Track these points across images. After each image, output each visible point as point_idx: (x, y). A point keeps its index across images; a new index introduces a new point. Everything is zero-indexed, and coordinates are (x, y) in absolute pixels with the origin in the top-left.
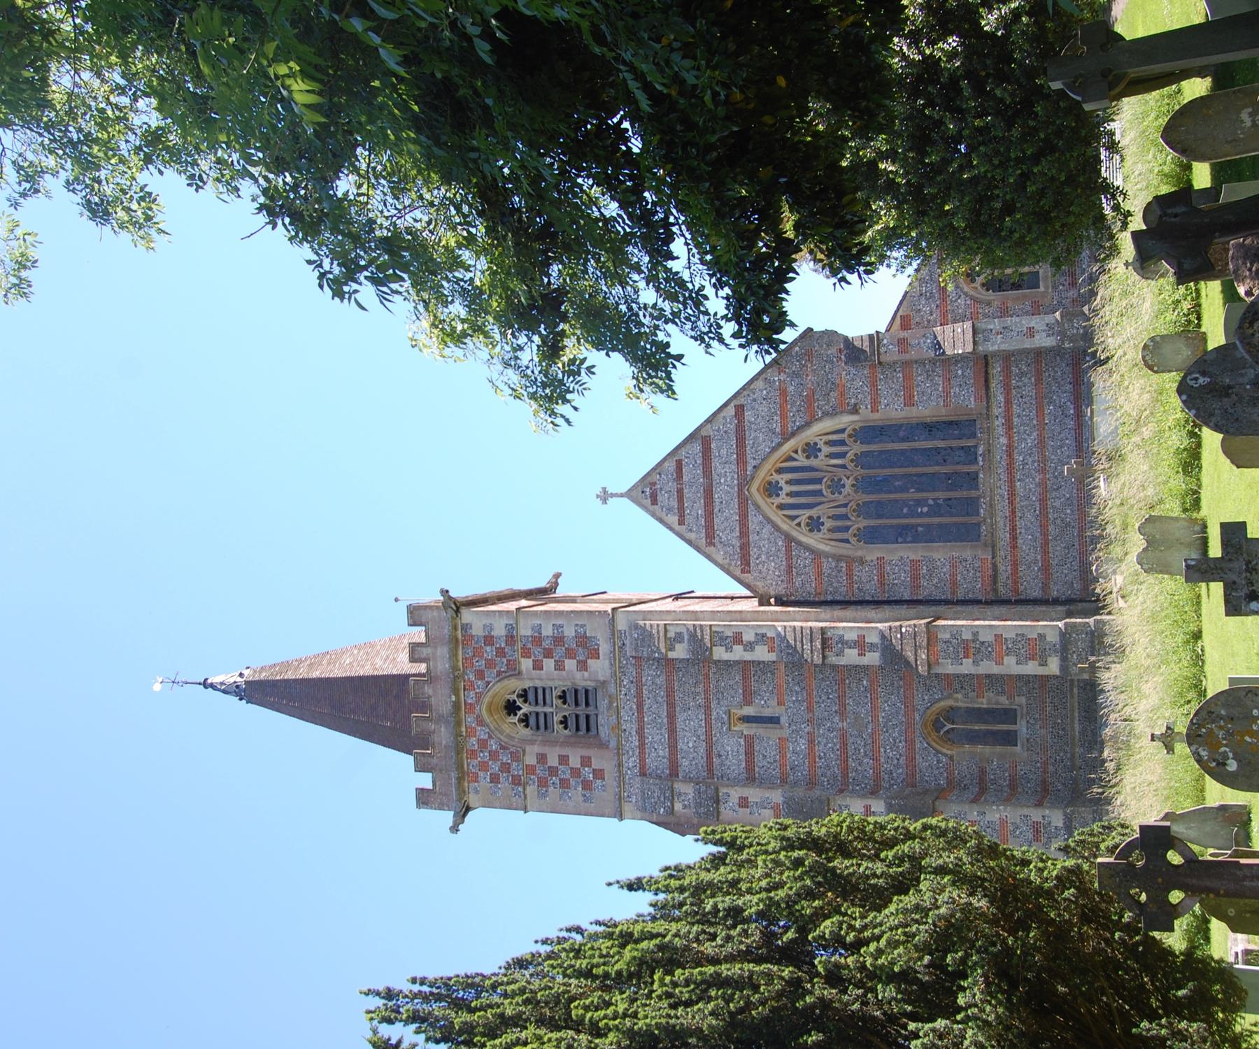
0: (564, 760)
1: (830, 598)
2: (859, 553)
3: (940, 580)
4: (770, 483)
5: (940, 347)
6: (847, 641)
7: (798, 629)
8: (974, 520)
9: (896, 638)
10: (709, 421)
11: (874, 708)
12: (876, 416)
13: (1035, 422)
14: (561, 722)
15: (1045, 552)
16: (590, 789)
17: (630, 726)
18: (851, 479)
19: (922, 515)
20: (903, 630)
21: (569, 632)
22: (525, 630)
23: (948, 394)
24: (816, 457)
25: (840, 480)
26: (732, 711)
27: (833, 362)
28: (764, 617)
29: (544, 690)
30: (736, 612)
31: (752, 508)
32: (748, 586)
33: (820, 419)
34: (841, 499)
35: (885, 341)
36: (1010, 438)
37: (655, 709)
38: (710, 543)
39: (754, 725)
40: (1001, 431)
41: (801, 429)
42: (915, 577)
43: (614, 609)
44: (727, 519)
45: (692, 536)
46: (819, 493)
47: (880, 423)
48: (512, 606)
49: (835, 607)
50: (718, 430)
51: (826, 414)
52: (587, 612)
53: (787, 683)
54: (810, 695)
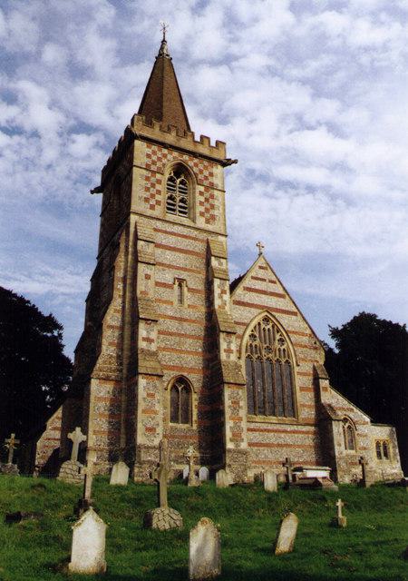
11: (189, 353)
37: (183, 244)
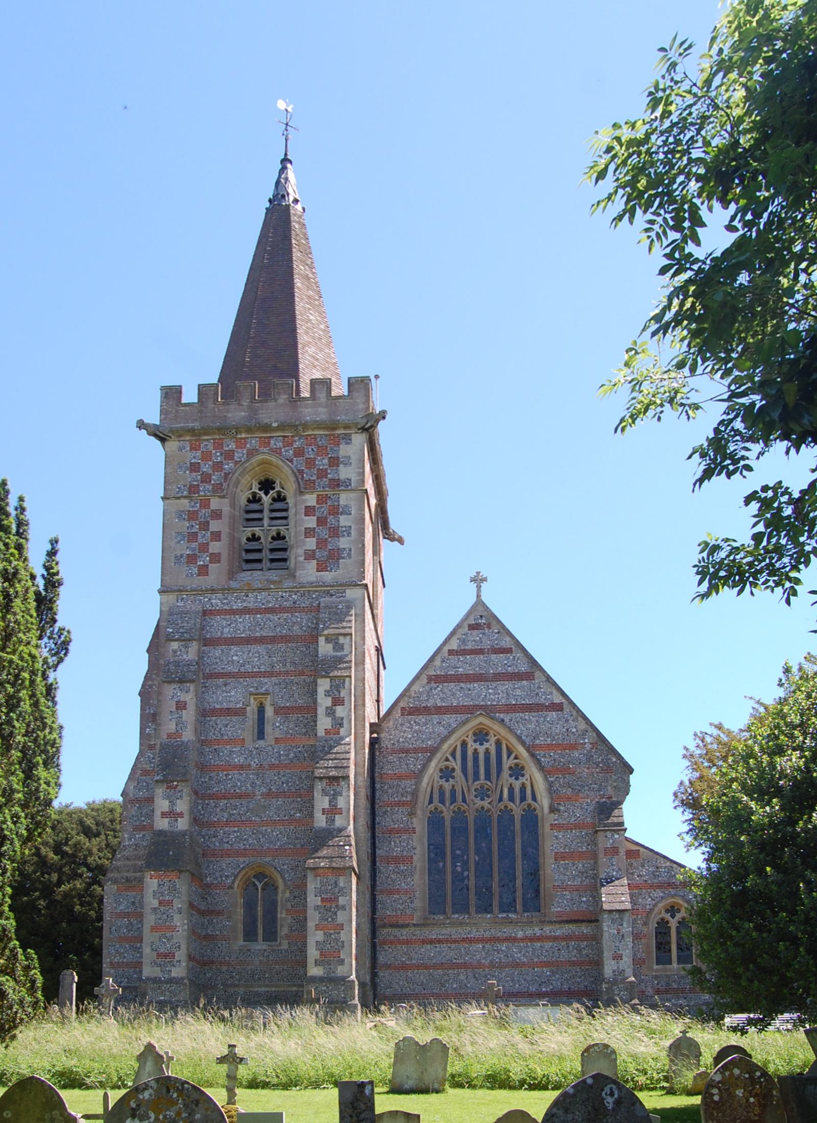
0: (216, 536)
1: (378, 786)
2: (419, 812)
3: (393, 881)
4: (487, 734)
5: (608, 883)
6: (336, 799)
7: (347, 756)
8: (449, 909)
9: (340, 841)
12: (547, 828)
13: (536, 960)
14: (254, 535)
15: (418, 967)
16: (188, 563)
17: (251, 601)
18: (489, 806)
19: (454, 865)
20: (347, 847)
21: (344, 543)
22: (344, 498)
23: (565, 889)
24: (511, 776)
25: (488, 796)
26: (269, 697)
27: (599, 791)
28: (359, 727)
29: (286, 518)
30: (364, 700)
31: (463, 718)
32: (389, 713)
33: (546, 779)
34: (470, 797)
35: (616, 836)
36: (522, 940)
37: (269, 625)
38: (430, 679)
39: (256, 717)
40: (529, 932)
41: (538, 762)
42: (397, 860)
43: (366, 586)
44: (454, 694)
45: (437, 663)
46: (476, 777)
47: (540, 831)
48: (369, 485)
49: (369, 790)
50: (539, 688)
51: (550, 785)
52: (364, 560)
53: (297, 747)
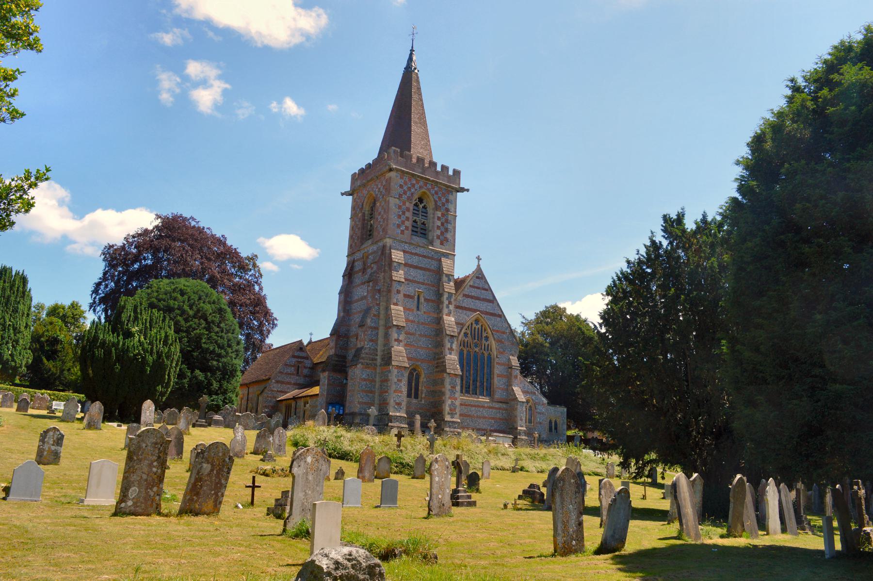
10: (498, 304)
36: (486, 407)
54: (427, 324)
